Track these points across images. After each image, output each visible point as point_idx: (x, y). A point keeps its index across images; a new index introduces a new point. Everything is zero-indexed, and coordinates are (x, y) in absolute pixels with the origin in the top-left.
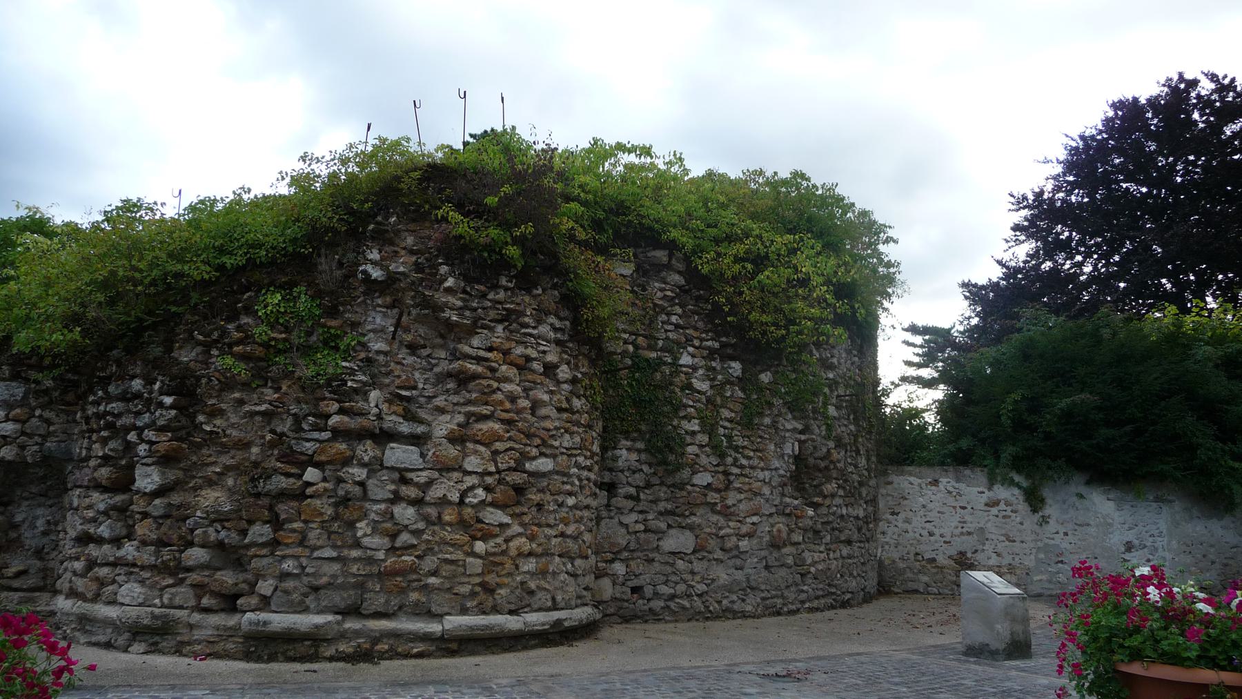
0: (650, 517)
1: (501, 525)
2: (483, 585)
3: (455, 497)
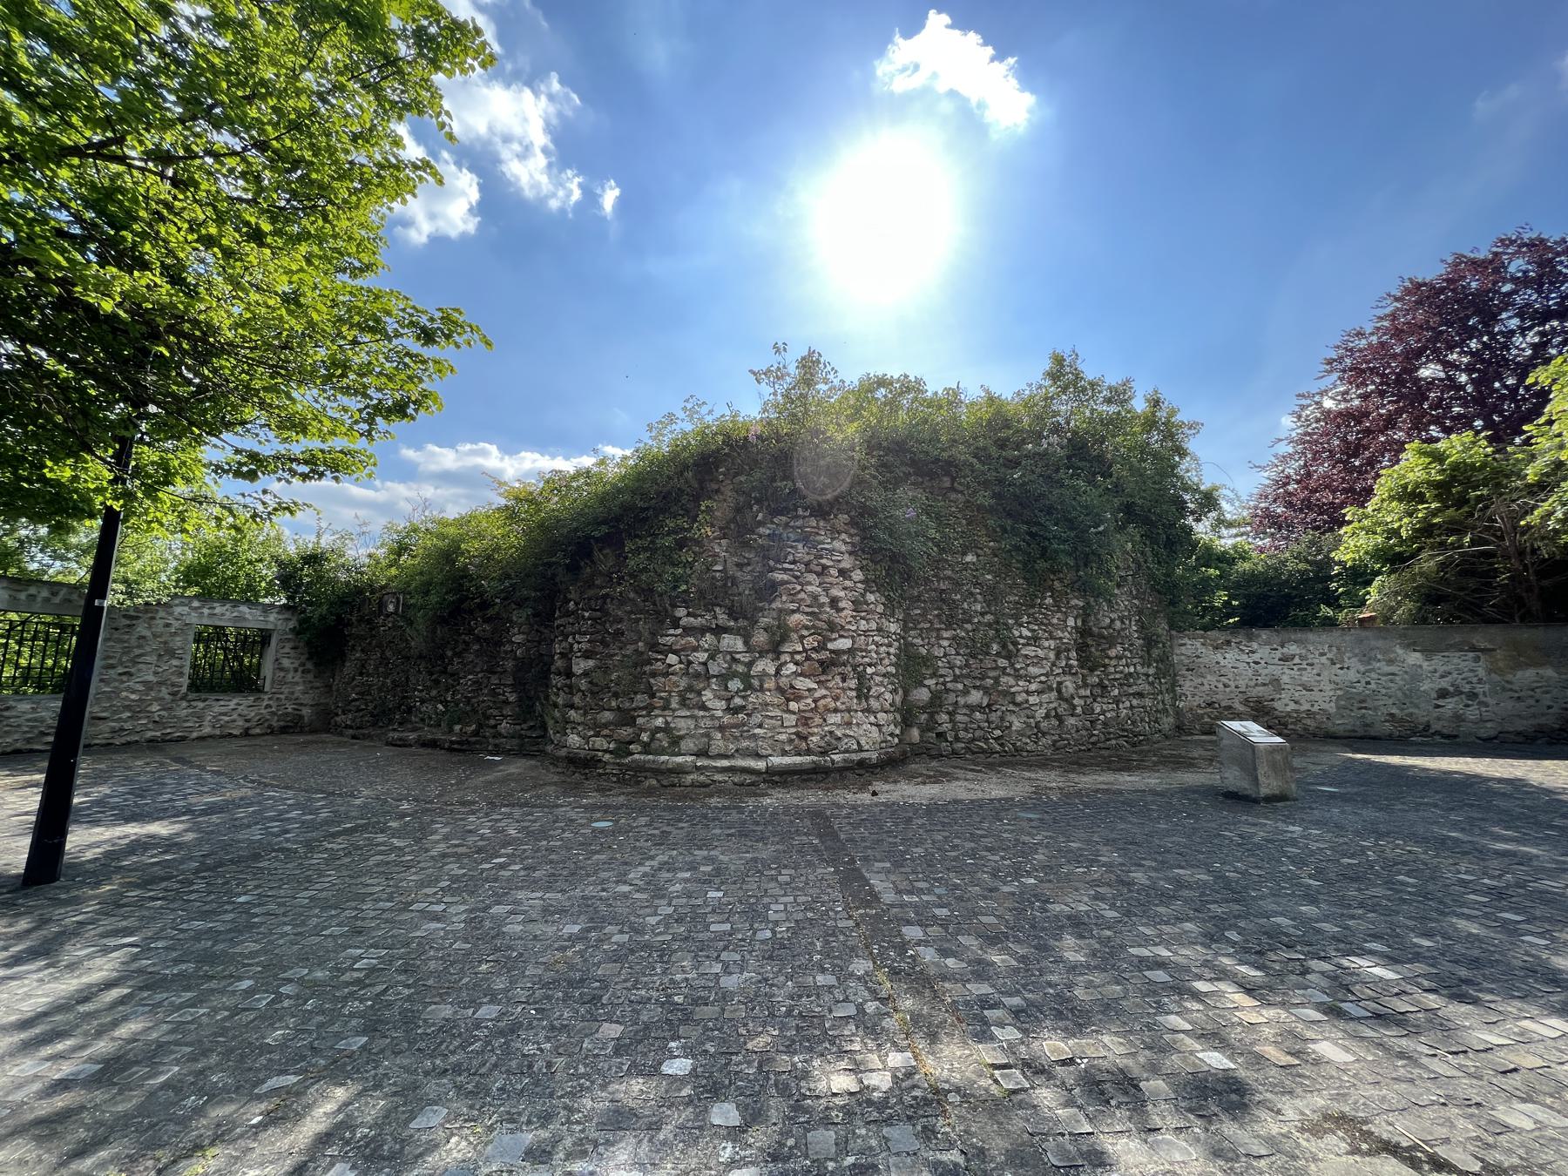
1: (809, 690)
3: (772, 671)
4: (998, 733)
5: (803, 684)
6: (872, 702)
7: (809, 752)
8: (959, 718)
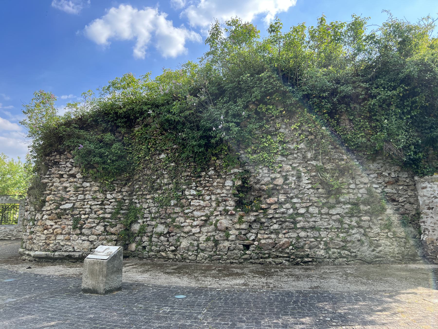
0: (148, 219)
4: (173, 248)
6: (83, 231)
7: (48, 250)
8: (153, 239)
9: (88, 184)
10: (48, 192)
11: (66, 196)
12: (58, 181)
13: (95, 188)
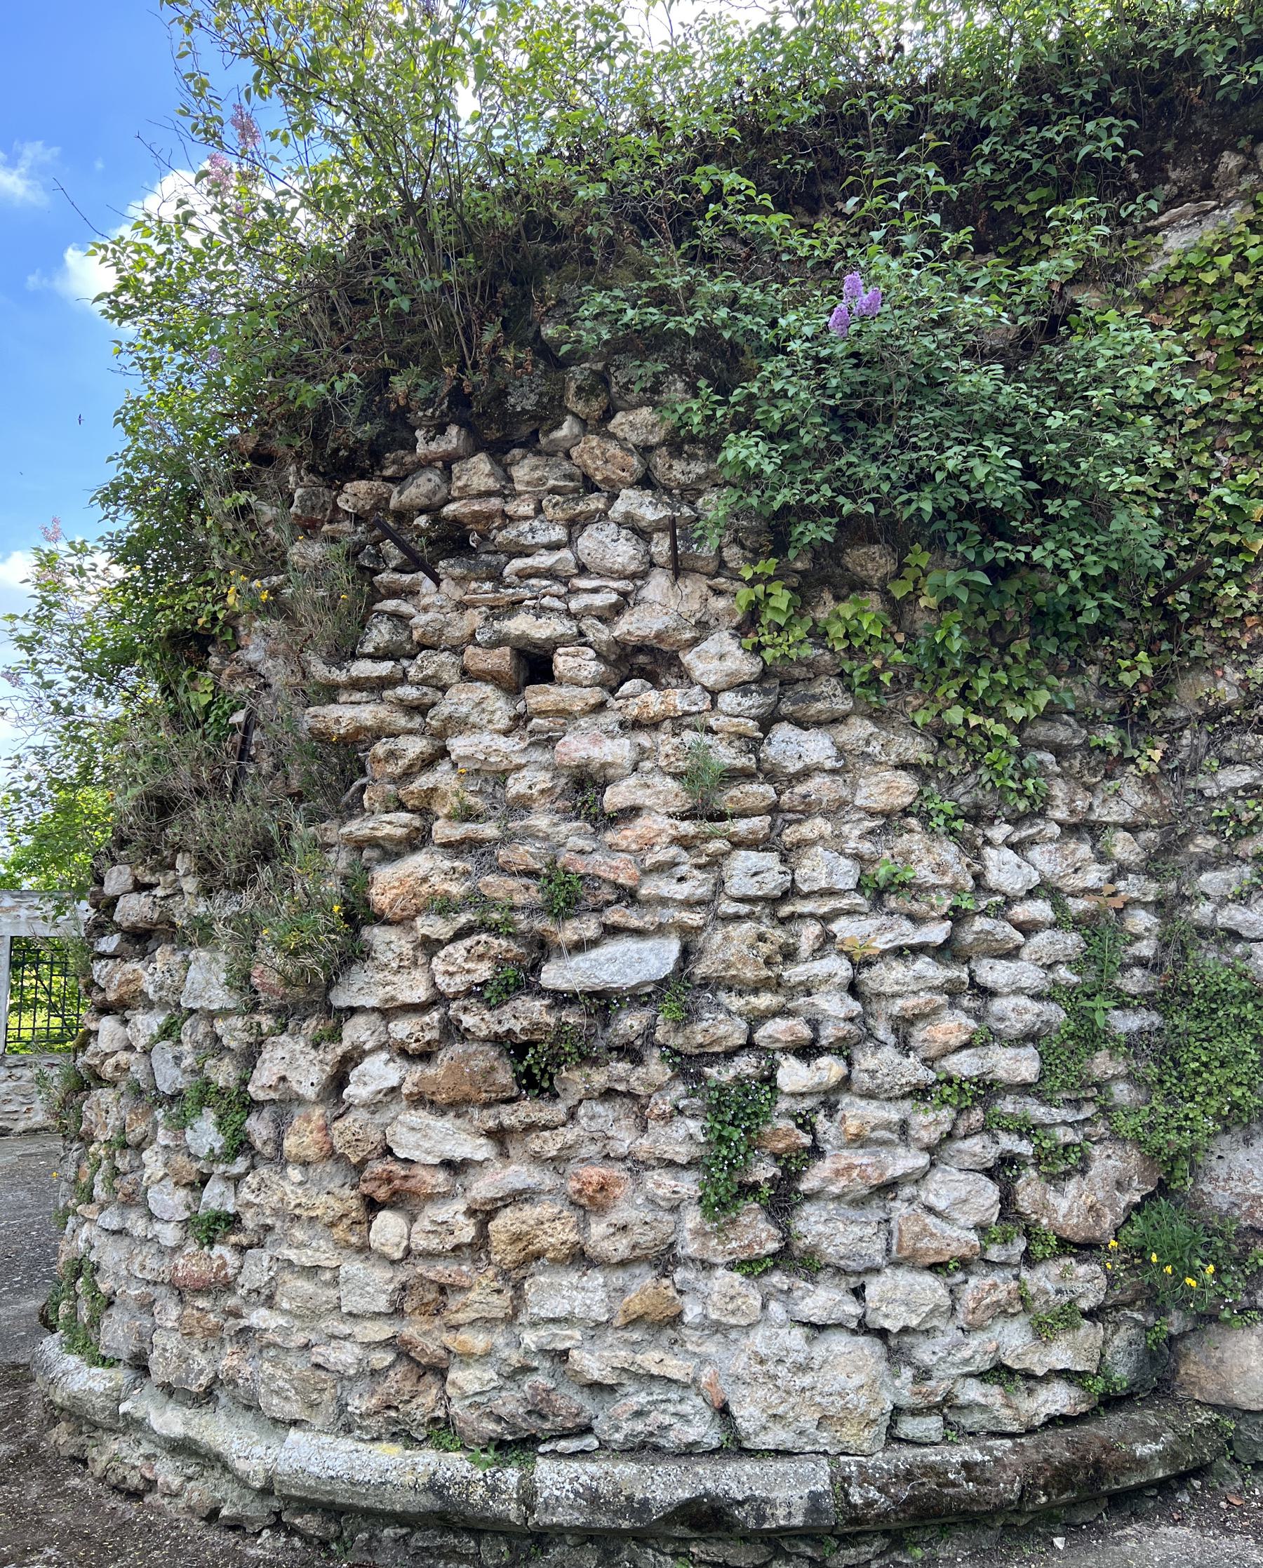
1: (449, 1165)
2: (402, 1350)
5: (427, 1138)
6: (812, 1224)
7: (442, 1430)
9: (817, 747)
10: (394, 825)
11: (600, 864)
12: (500, 708)
13: (888, 788)
